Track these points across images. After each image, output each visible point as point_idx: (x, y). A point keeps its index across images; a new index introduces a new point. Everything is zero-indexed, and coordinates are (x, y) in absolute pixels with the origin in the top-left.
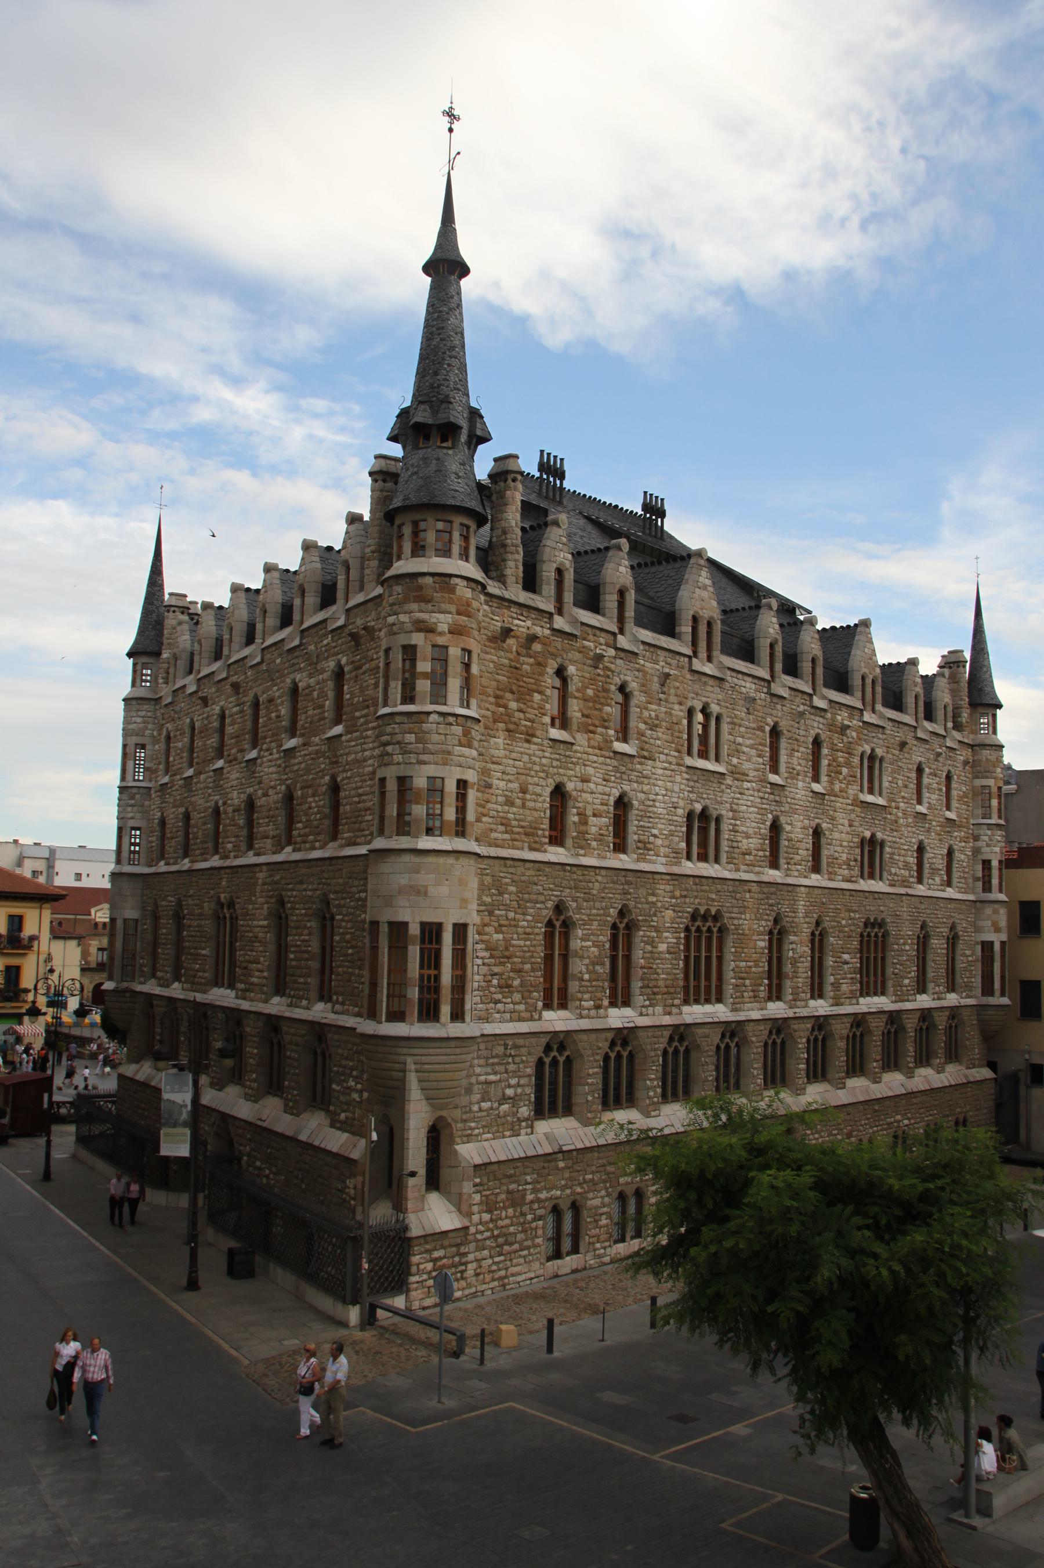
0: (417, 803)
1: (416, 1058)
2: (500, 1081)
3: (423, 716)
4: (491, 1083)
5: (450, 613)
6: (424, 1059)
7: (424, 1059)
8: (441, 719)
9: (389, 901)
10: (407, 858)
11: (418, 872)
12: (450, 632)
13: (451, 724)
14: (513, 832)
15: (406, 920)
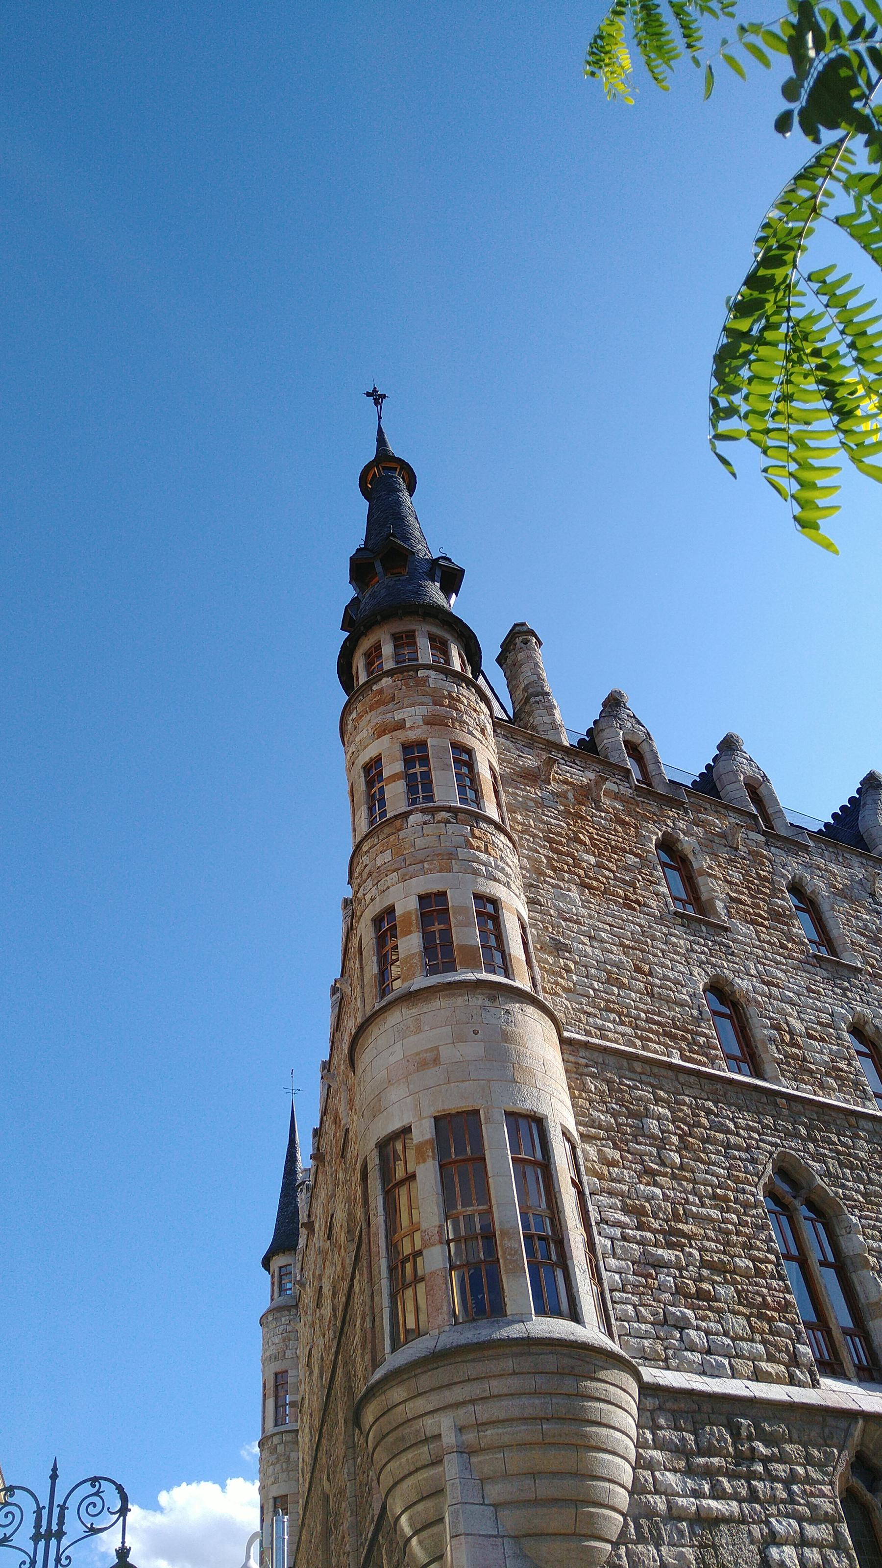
0: (410, 932)
1: (461, 1412)
2: (743, 1520)
3: (398, 823)
4: (715, 1521)
5: (422, 704)
6: (484, 1412)
7: (484, 1412)
8: (427, 818)
9: (376, 1110)
10: (395, 1017)
11: (419, 1030)
12: (427, 723)
13: (448, 822)
14: (637, 1027)
15: (405, 1122)
